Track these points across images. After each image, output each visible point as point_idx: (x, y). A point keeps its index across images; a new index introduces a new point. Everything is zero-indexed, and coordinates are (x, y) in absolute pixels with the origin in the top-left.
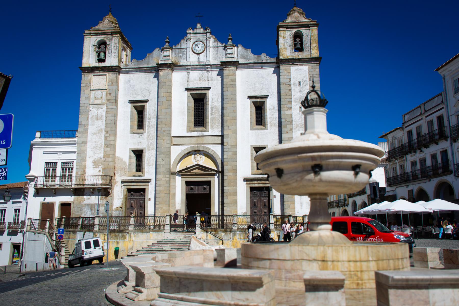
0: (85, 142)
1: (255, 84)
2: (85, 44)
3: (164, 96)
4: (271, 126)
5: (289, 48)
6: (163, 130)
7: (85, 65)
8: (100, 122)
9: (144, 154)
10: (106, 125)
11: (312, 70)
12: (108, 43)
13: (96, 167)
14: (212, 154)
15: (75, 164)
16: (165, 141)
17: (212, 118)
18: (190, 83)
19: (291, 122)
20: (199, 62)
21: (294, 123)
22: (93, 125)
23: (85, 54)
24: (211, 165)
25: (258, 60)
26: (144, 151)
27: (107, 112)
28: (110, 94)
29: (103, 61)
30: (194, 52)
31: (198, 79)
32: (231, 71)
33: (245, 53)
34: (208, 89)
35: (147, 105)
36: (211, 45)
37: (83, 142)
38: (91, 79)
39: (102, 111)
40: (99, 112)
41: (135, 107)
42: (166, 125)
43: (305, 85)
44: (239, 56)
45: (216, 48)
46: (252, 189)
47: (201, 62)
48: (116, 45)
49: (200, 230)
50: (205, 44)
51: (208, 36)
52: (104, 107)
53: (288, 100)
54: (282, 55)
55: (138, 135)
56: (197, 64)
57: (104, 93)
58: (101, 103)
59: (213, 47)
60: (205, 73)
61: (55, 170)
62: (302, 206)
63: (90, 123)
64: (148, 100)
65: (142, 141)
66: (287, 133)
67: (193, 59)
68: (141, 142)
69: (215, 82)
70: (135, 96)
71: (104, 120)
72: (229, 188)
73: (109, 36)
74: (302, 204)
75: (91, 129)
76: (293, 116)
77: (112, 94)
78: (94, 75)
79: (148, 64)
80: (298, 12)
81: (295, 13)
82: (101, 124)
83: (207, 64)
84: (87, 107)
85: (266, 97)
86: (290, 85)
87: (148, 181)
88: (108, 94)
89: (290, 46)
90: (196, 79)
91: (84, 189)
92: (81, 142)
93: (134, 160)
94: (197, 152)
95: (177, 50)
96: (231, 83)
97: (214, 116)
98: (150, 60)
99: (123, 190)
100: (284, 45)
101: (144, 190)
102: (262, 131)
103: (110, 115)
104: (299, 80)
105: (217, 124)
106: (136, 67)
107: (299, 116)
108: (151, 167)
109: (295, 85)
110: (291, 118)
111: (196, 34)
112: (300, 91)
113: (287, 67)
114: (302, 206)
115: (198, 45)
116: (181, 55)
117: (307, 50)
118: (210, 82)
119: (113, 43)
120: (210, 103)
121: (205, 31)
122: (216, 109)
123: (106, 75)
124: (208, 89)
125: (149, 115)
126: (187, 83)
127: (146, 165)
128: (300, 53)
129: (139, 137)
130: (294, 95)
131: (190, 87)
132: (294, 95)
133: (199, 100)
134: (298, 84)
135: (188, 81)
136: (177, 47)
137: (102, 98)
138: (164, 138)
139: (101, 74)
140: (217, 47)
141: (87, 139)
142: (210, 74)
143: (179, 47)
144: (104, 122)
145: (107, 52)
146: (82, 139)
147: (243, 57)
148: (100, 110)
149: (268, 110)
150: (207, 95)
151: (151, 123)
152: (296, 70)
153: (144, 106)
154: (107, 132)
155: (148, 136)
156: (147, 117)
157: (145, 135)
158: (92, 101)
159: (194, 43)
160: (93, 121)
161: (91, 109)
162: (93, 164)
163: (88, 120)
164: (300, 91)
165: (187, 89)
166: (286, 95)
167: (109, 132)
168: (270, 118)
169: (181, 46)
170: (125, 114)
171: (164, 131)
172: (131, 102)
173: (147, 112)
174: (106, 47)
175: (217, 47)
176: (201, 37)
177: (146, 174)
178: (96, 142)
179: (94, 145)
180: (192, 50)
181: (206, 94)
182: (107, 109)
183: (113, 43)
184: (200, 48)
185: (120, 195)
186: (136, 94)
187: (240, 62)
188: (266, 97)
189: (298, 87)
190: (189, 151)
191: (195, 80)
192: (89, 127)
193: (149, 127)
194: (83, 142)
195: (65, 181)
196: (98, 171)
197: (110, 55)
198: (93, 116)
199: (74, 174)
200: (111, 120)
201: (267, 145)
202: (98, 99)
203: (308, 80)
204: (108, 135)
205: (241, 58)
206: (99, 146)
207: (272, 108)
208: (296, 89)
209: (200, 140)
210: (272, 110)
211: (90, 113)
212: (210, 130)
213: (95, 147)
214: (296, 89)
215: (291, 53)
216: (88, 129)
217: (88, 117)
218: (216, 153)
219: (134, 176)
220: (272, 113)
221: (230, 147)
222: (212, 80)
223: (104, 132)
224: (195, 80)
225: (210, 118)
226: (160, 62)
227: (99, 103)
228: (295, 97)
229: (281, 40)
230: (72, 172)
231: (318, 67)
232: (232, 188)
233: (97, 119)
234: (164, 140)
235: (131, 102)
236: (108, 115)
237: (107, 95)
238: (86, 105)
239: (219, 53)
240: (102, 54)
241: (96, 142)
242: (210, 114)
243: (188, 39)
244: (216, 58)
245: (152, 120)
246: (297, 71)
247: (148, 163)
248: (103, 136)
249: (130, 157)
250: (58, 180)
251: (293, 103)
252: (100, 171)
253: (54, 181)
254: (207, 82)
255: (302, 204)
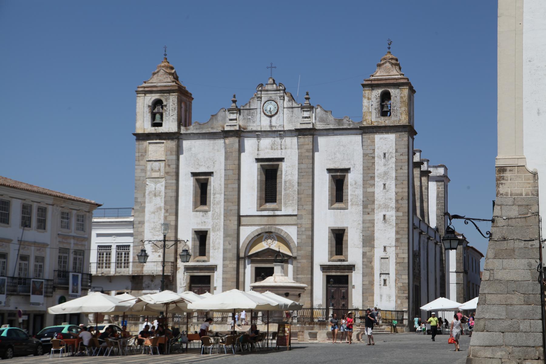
0: (142, 223)
1: (335, 154)
2: (138, 104)
3: (231, 168)
4: (352, 205)
5: (374, 111)
6: (229, 208)
7: (139, 131)
8: (158, 198)
9: (208, 236)
10: (166, 203)
11: (400, 139)
12: (165, 103)
13: (156, 251)
14: (285, 236)
15: (131, 249)
16: (232, 221)
17: (285, 194)
18: (260, 152)
19: (373, 202)
20: (271, 126)
21: (376, 202)
22: (150, 202)
23: (139, 117)
24: (284, 250)
25: (339, 125)
26: (208, 233)
27: (166, 187)
28: (169, 166)
29: (160, 125)
30: (265, 114)
31: (269, 147)
32: (307, 139)
33: (324, 116)
34: (281, 160)
35: (212, 179)
36: (285, 106)
37: (139, 223)
38: (146, 148)
39: (161, 186)
40: (157, 187)
41: (197, 180)
42: (232, 203)
43: (391, 158)
44: (317, 119)
45: (291, 110)
46: (328, 278)
47: (274, 126)
48: (174, 106)
49: (261, 323)
50: (278, 103)
51: (282, 94)
52: (163, 182)
53: (371, 175)
54: (366, 120)
55: (201, 213)
56: (269, 129)
57: (163, 164)
58: (158, 176)
59: (287, 108)
60: (278, 140)
61: (110, 254)
62: (381, 298)
63: (147, 200)
64: (212, 173)
65: (206, 220)
66: (369, 214)
67: (263, 123)
68: (205, 222)
69: (289, 151)
70: (197, 166)
71: (163, 197)
72: (302, 276)
73: (165, 94)
74: (381, 296)
75: (149, 207)
76: (376, 195)
77: (171, 166)
78: (150, 143)
79: (212, 128)
80: (389, 62)
81: (386, 63)
82: (160, 202)
83: (280, 129)
84: (144, 180)
85: (347, 170)
86: (374, 158)
87: (213, 268)
88: (167, 166)
89: (375, 109)
90: (267, 148)
91: (142, 276)
92: (137, 223)
93: (198, 243)
94: (268, 234)
95: (246, 112)
96: (307, 154)
97: (288, 192)
98: (215, 123)
99: (185, 277)
100: (368, 109)
101: (209, 277)
102: (342, 211)
103: (170, 191)
104: (384, 152)
105: (291, 202)
106: (197, 132)
107: (382, 194)
108: (216, 251)
109: (379, 157)
110: (374, 196)
111: (267, 91)
112: (385, 165)
113: (371, 136)
114: (381, 298)
115: (268, 109)
116: (250, 117)
117: (395, 114)
118: (283, 151)
119: (171, 104)
120: (283, 176)
121: (278, 88)
122: (290, 183)
123: (163, 143)
124: (281, 160)
125: (214, 189)
126: (256, 152)
127: (211, 248)
128: (386, 118)
129: (203, 216)
130: (378, 170)
131: (260, 157)
132: (378, 170)
133: (270, 172)
134: (382, 156)
135: (258, 150)
136: (245, 108)
137: (159, 170)
138: (230, 218)
139: (158, 141)
140: (292, 108)
141: (144, 219)
142: (284, 140)
143: (248, 107)
144: (163, 199)
145: (164, 114)
146: (139, 219)
147: (322, 120)
148: (159, 185)
149: (349, 187)
150: (280, 167)
151: (217, 200)
152: (381, 138)
153: (208, 179)
154: (167, 211)
155: (213, 214)
156: (212, 192)
157: (210, 213)
158: (148, 174)
159: (265, 102)
160: (151, 198)
161: (147, 183)
162: (152, 248)
163: (144, 196)
164: (385, 165)
165: (258, 160)
166: (369, 169)
167: (169, 211)
168: (351, 195)
169: (250, 106)
170: (187, 187)
171: (231, 210)
172: (194, 174)
173: (212, 186)
174: (162, 108)
175: (292, 108)
176: (272, 95)
177: (211, 260)
178: (154, 223)
179: (153, 226)
180: (263, 112)
181: (278, 165)
182: (166, 183)
183: (171, 104)
184: (271, 107)
185: (182, 283)
186: (198, 164)
187: (319, 126)
188: (347, 170)
189: (383, 160)
190: (260, 232)
191: (266, 148)
192: (147, 205)
193: (214, 204)
194: (139, 223)
195: (121, 267)
196: (157, 256)
197: (167, 118)
198: (150, 192)
199: (131, 259)
200: (171, 197)
201: (347, 227)
202: (155, 171)
203: (394, 151)
204: (167, 214)
205: (319, 122)
206: (158, 227)
207: (354, 183)
208: (380, 162)
209: (271, 220)
210: (354, 186)
211: (147, 188)
212: (283, 208)
213: (154, 228)
214: (380, 162)
215: (376, 117)
216: (144, 207)
217: (144, 193)
218: (290, 236)
219: (198, 261)
220: (354, 189)
221: (304, 229)
222: (286, 148)
223: (163, 211)
224: (266, 148)
225: (283, 194)
226: (227, 129)
227: (156, 176)
228: (379, 172)
229: (365, 102)
230: (128, 257)
231: (407, 135)
232: (305, 276)
233: (155, 195)
234: (230, 221)
235: (194, 174)
236: (168, 191)
237: (165, 167)
238: (142, 178)
239: (294, 115)
240: (158, 116)
241: (154, 223)
242: (283, 190)
243: (258, 98)
244: (290, 121)
245: (217, 196)
246: (382, 140)
247: (213, 247)
248: (162, 215)
249: (194, 239)
250: (113, 265)
251: (376, 179)
252: (159, 256)
253: (109, 267)
254: (280, 151)
255: (381, 296)
